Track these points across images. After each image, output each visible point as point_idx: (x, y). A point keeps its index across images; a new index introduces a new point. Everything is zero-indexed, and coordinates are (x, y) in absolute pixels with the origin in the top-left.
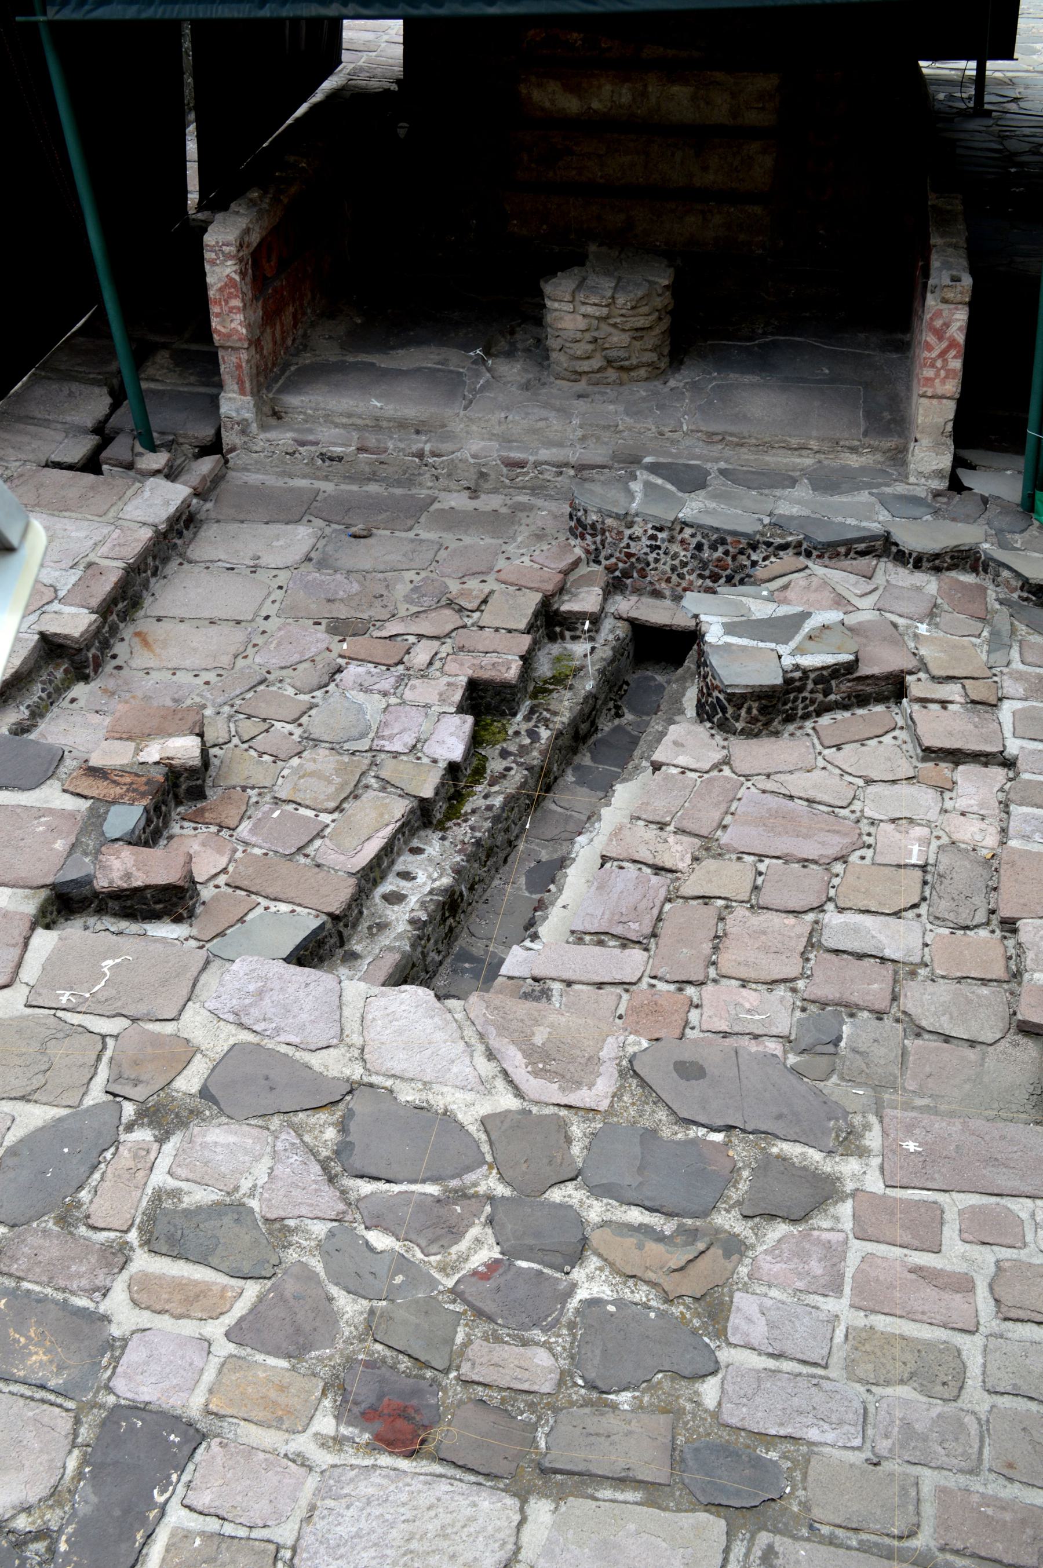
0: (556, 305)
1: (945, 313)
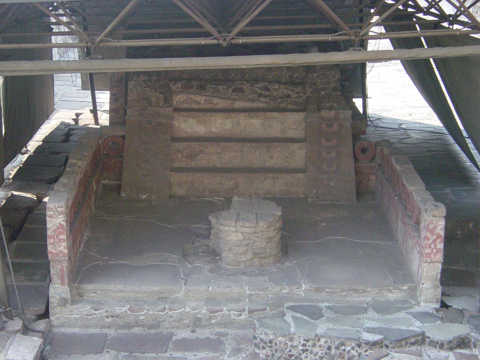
0: (227, 228)
1: (434, 222)
